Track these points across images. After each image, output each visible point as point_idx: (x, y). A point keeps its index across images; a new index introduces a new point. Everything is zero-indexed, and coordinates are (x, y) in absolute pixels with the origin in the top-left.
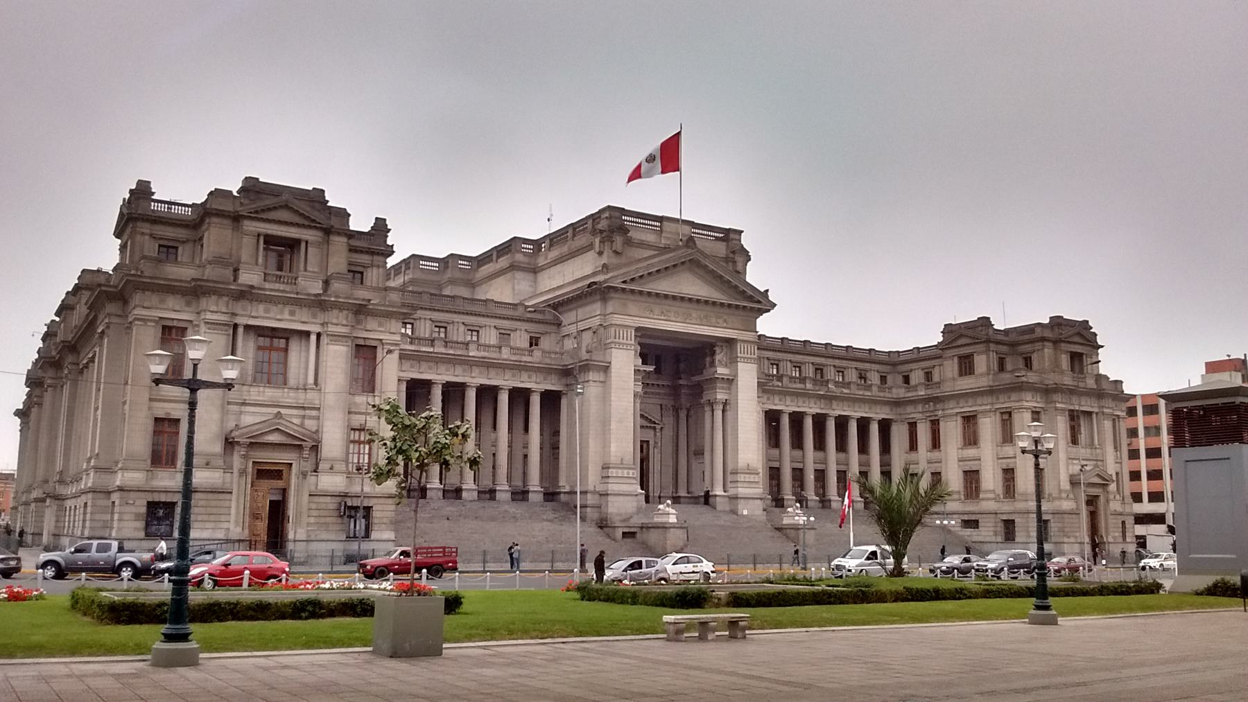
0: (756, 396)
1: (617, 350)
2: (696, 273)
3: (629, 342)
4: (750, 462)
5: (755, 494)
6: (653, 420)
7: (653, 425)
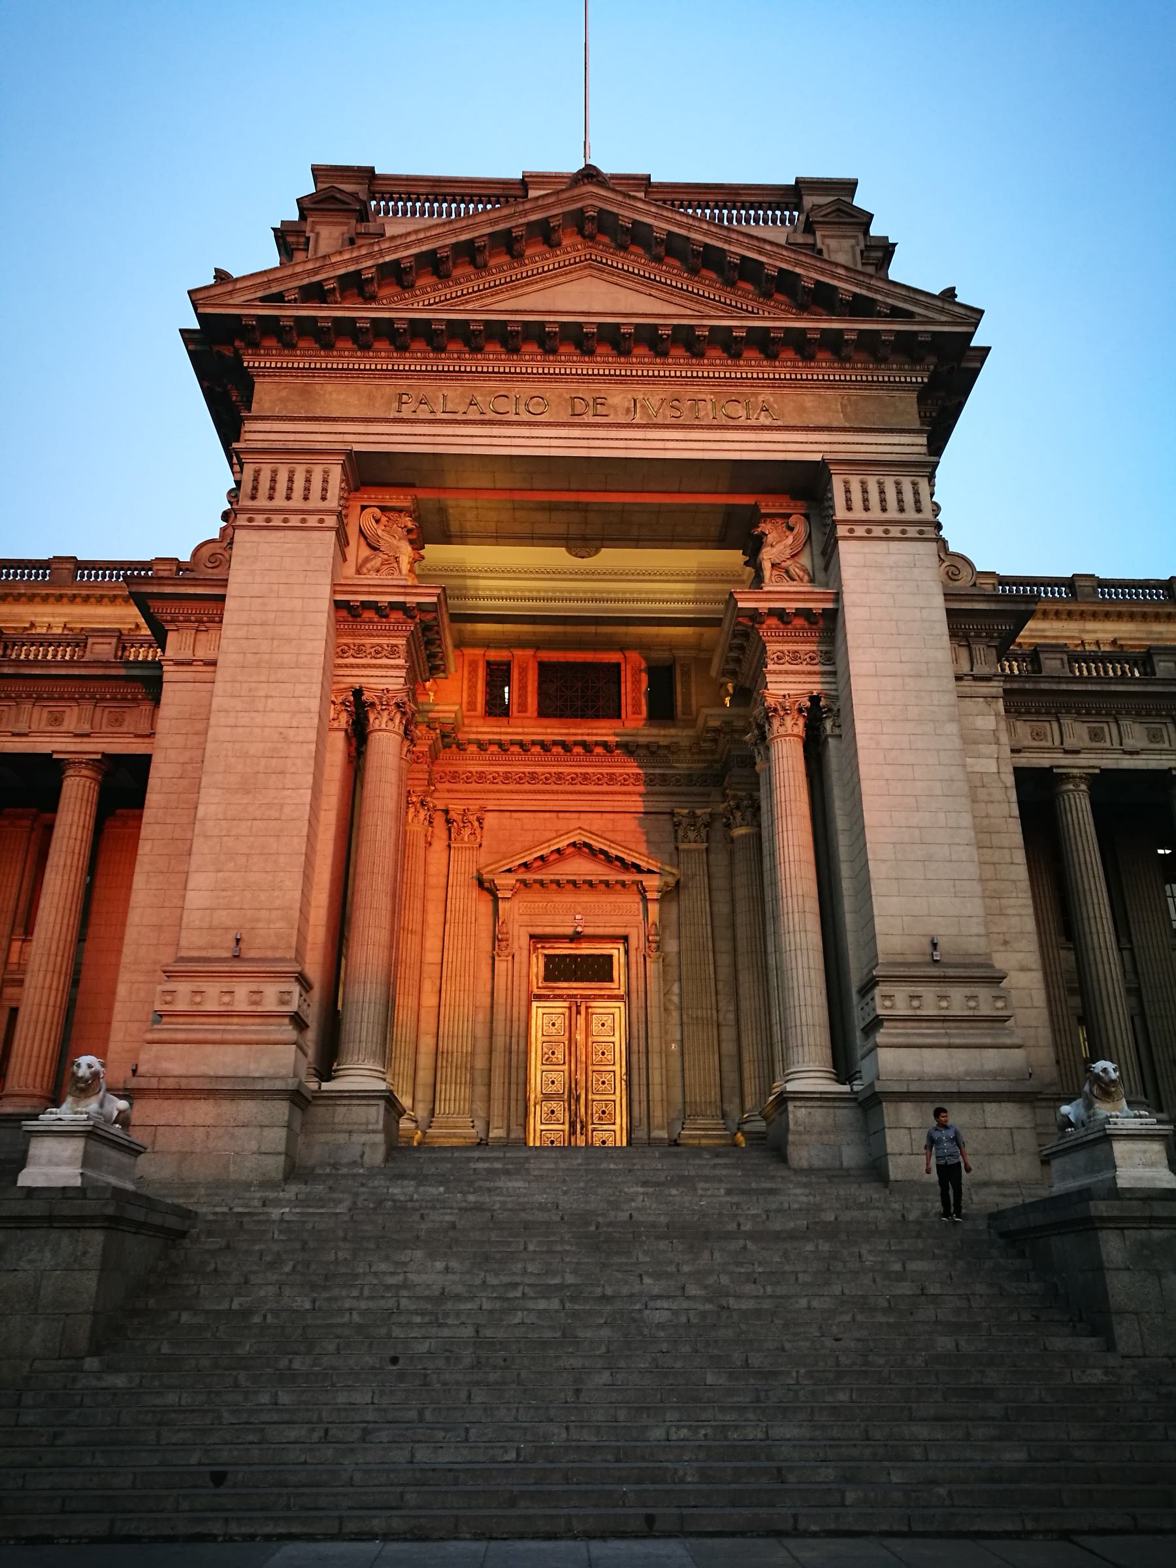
0: (949, 671)
1: (254, 536)
2: (614, 271)
3: (315, 502)
4: (944, 931)
5: (994, 1075)
6: (629, 859)
7: (627, 877)
